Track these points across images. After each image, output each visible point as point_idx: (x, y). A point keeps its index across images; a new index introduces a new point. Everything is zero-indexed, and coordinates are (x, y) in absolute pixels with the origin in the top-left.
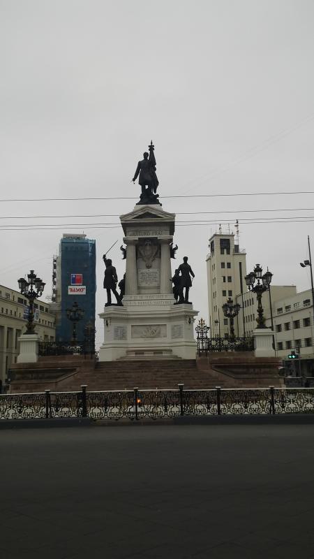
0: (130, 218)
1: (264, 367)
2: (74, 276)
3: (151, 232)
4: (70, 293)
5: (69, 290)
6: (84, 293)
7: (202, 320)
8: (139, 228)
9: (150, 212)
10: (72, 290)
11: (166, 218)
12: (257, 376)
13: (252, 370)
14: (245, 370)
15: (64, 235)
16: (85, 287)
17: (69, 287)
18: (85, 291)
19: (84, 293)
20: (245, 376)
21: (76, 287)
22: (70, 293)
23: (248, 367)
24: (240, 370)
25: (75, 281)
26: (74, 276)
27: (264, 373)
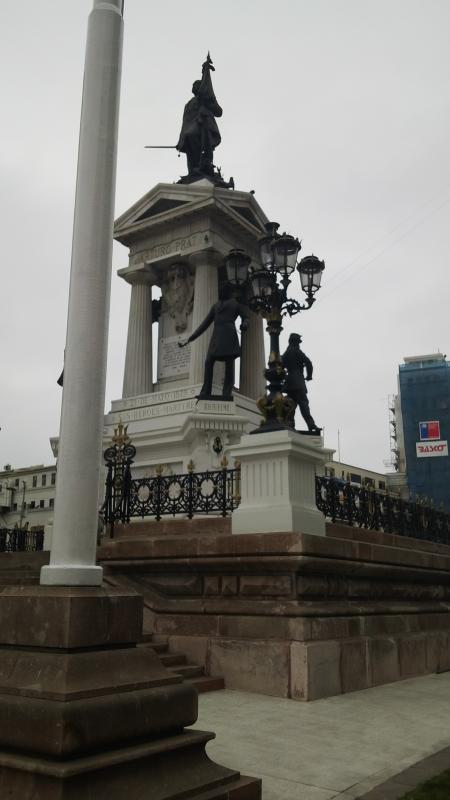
0: (129, 223)
1: (253, 570)
2: (424, 424)
3: (173, 244)
4: (420, 454)
5: (418, 450)
6: (445, 452)
7: (121, 427)
8: (149, 243)
9: (165, 196)
10: (422, 450)
11: (197, 200)
12: (225, 605)
13: (210, 583)
14: (189, 583)
15: (406, 360)
16: (445, 442)
17: (418, 444)
18: (446, 449)
19: (445, 452)
20: (190, 604)
21: (429, 444)
22: (420, 454)
23: (201, 571)
24: (176, 583)
25: (427, 433)
26: (424, 424)
27: (253, 593)
